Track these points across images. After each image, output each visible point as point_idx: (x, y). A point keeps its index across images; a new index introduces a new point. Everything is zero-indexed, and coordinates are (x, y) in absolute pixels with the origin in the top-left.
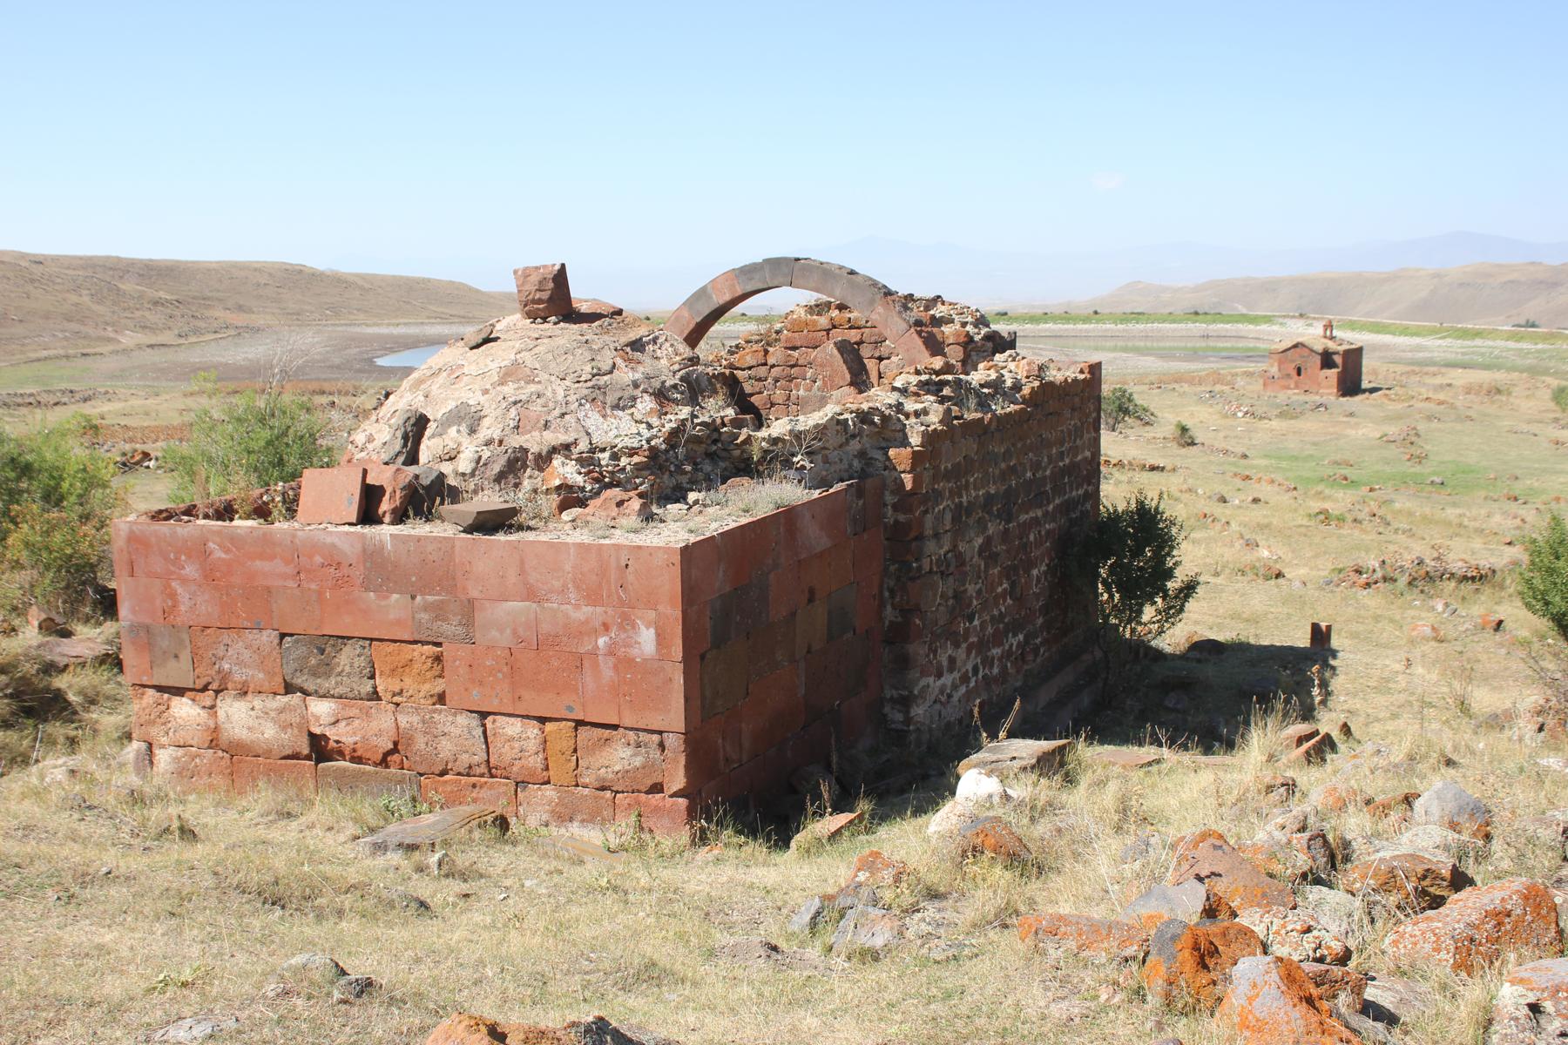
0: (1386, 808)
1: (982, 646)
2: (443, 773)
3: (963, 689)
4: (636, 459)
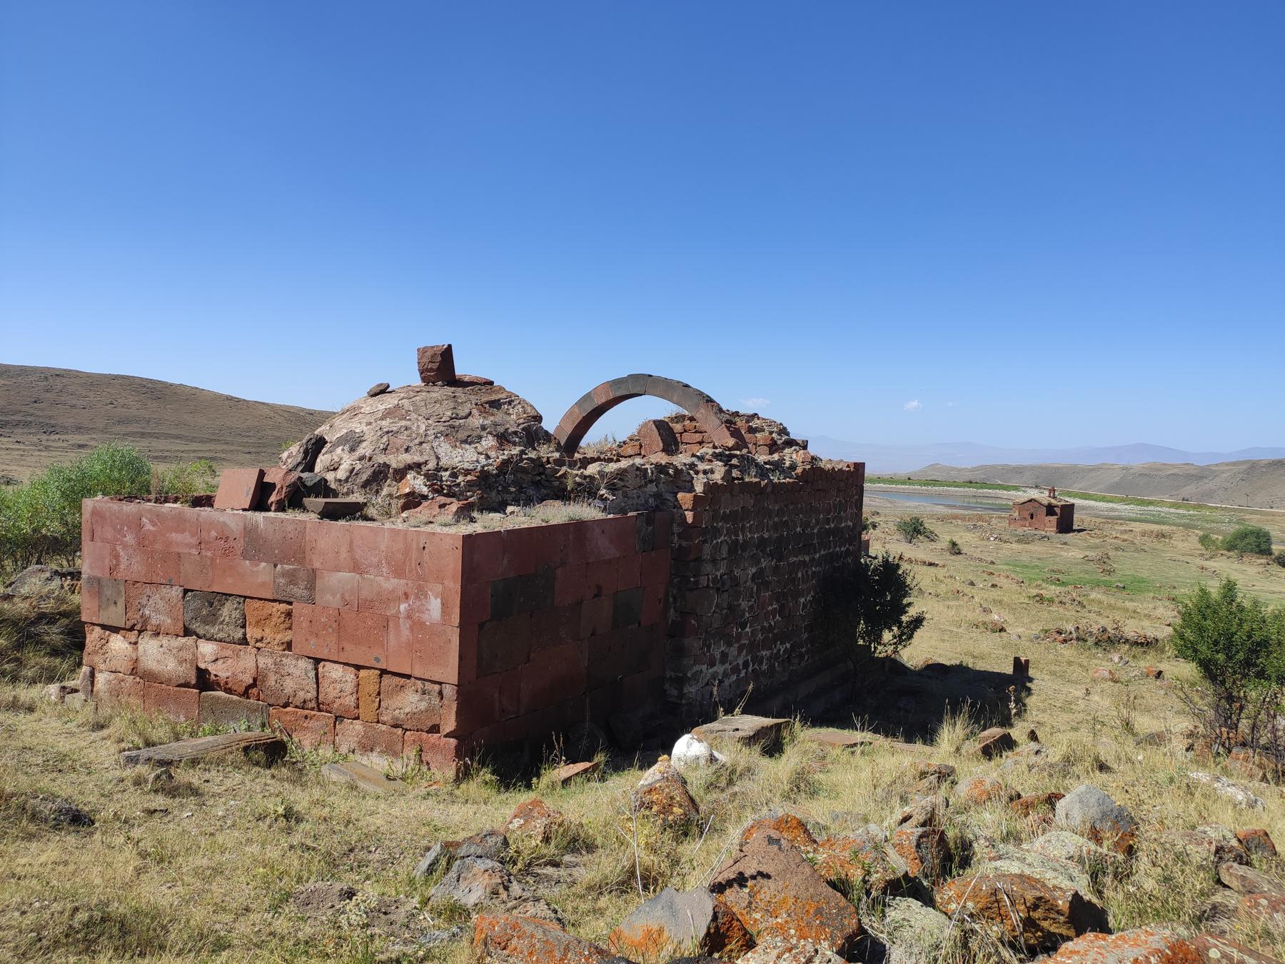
0: (1028, 807)
1: (753, 647)
2: (286, 705)
3: (734, 678)
4: (469, 478)
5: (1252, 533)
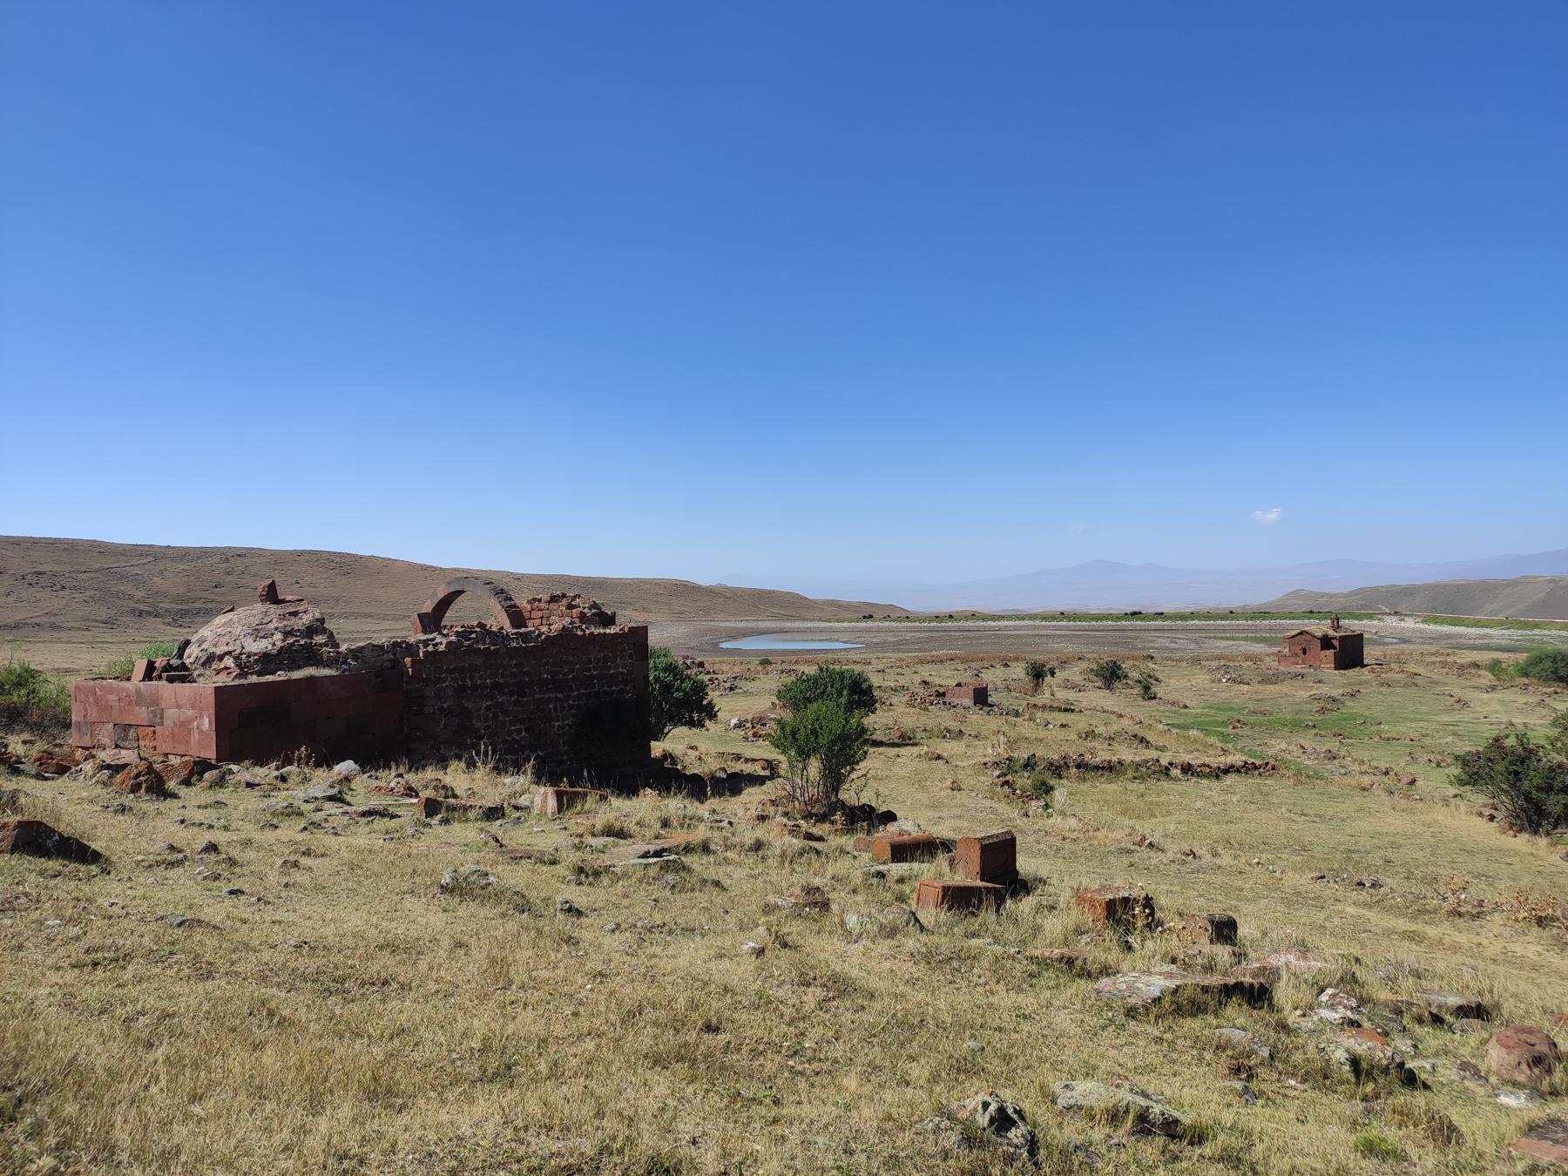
5: (1548, 657)
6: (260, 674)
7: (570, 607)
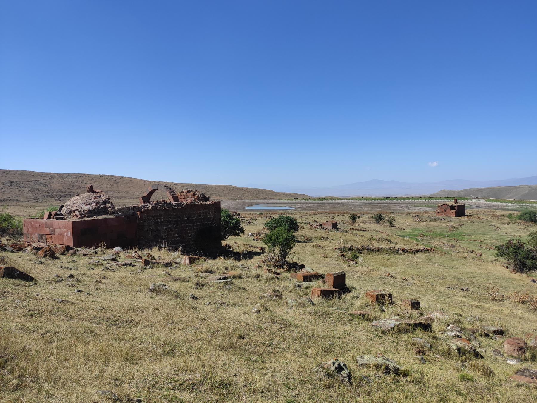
5: (528, 213)
6: (88, 217)
7: (194, 195)
